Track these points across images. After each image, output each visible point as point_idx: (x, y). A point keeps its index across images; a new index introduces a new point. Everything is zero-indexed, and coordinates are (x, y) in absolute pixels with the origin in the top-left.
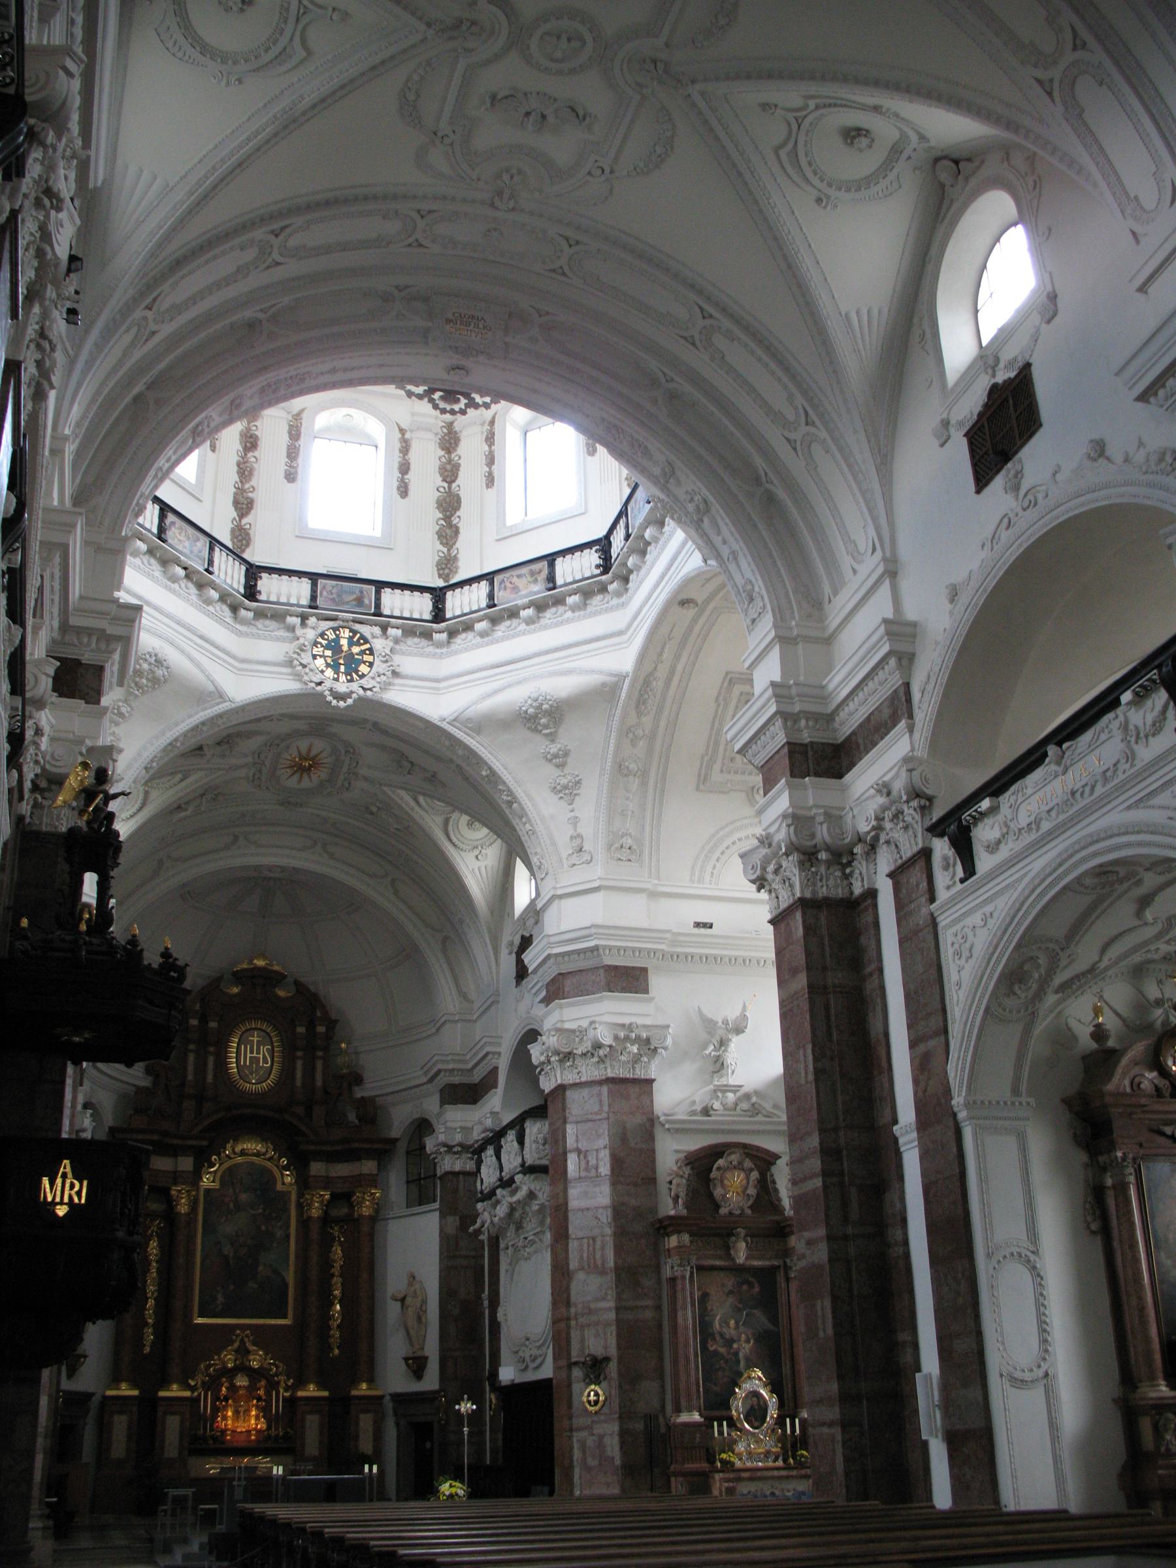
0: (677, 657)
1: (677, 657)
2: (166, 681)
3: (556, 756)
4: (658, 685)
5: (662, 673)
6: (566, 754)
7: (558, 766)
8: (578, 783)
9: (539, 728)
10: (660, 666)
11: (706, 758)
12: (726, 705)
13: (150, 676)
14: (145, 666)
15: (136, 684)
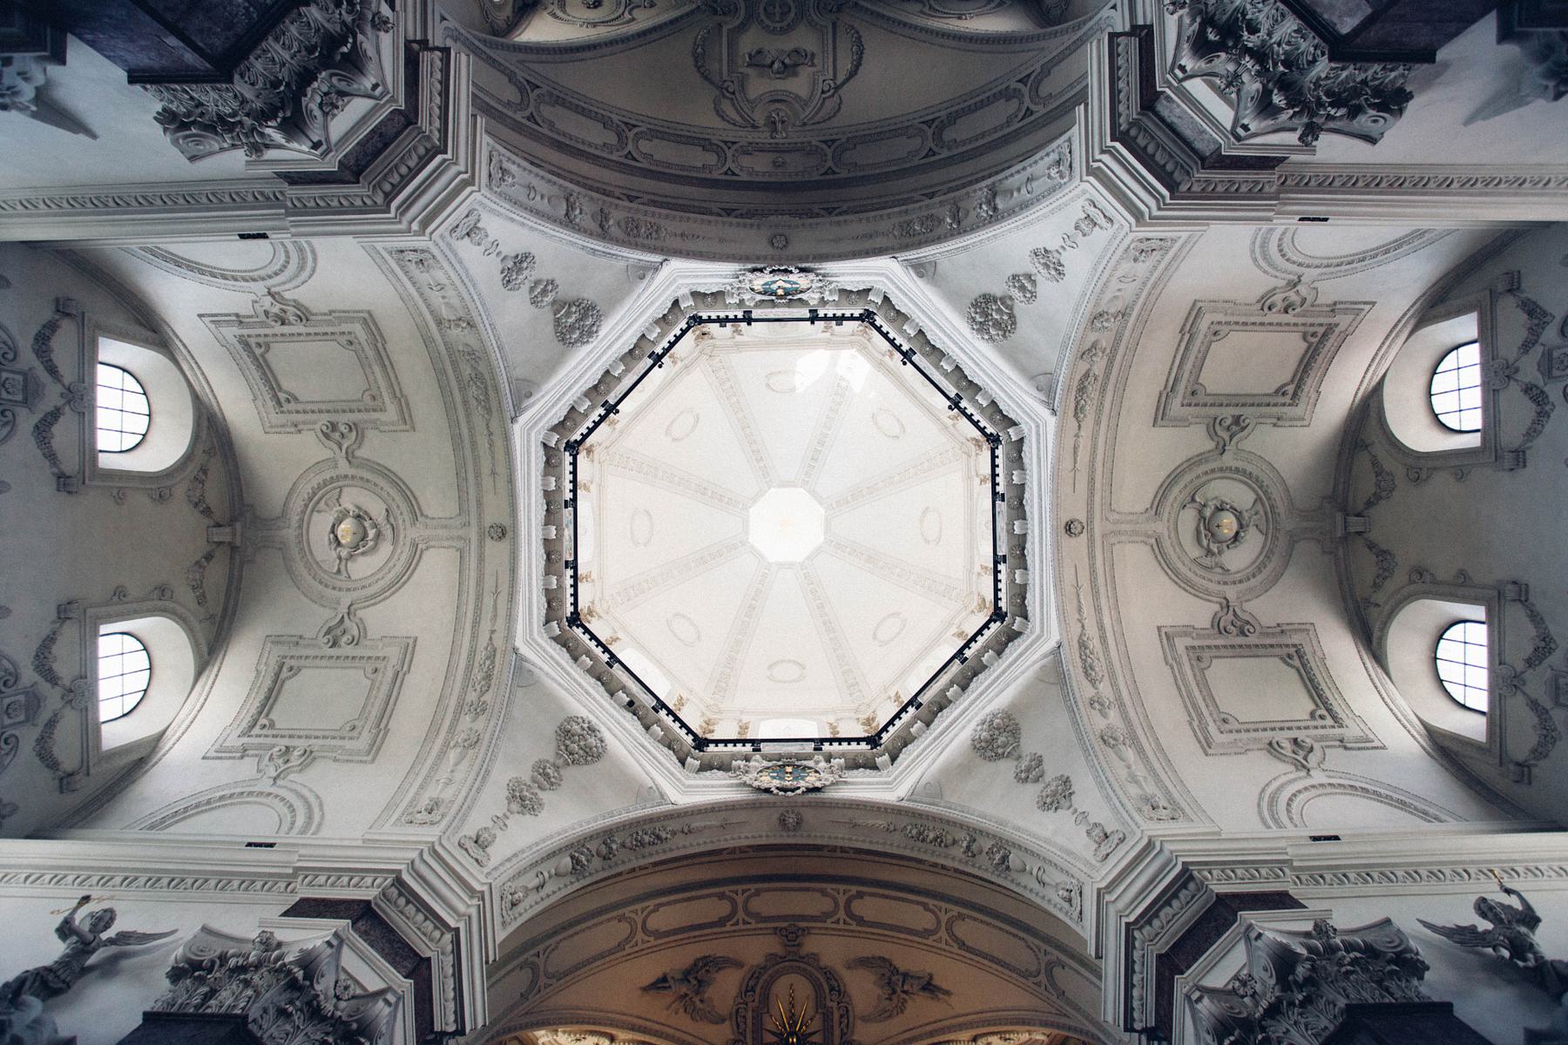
0: (1098, 610)
1: (1098, 610)
2: (599, 756)
3: (1028, 770)
4: (1095, 644)
5: (1092, 631)
6: (1039, 761)
7: (1037, 780)
8: (1066, 782)
9: (1000, 751)
10: (1086, 622)
11: (1195, 724)
12: (1179, 664)
13: (582, 743)
14: (576, 728)
15: (567, 746)
